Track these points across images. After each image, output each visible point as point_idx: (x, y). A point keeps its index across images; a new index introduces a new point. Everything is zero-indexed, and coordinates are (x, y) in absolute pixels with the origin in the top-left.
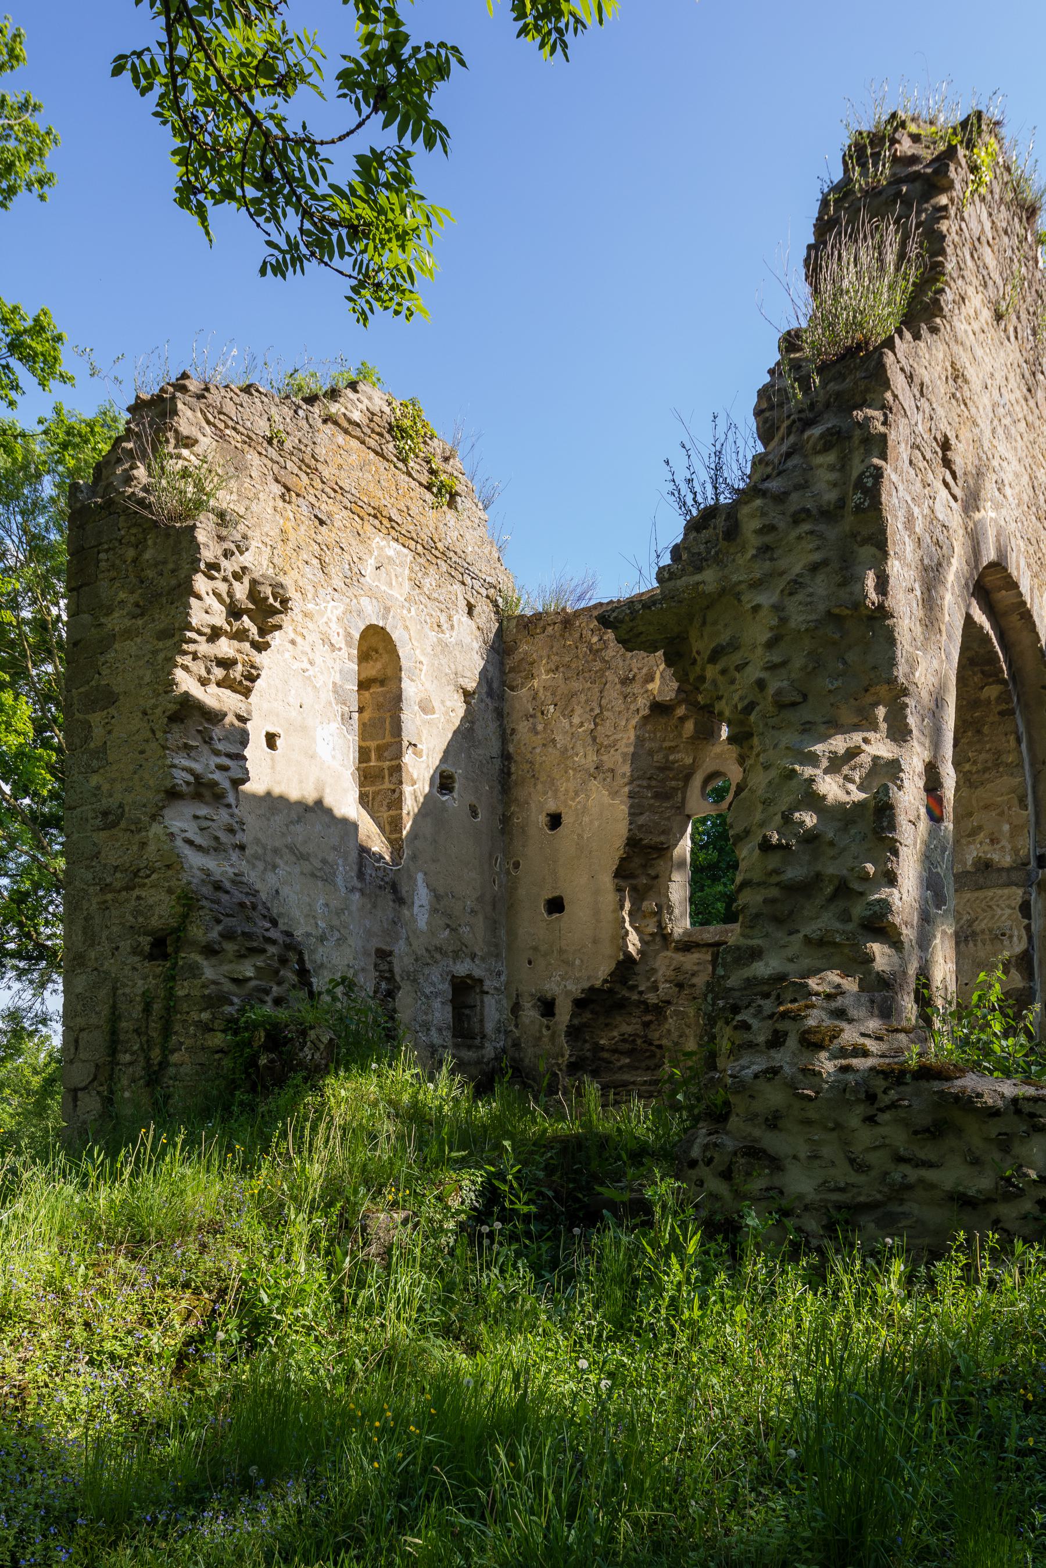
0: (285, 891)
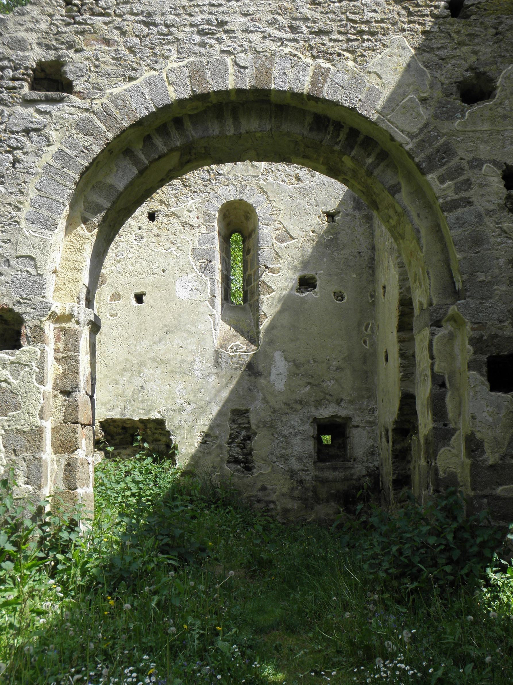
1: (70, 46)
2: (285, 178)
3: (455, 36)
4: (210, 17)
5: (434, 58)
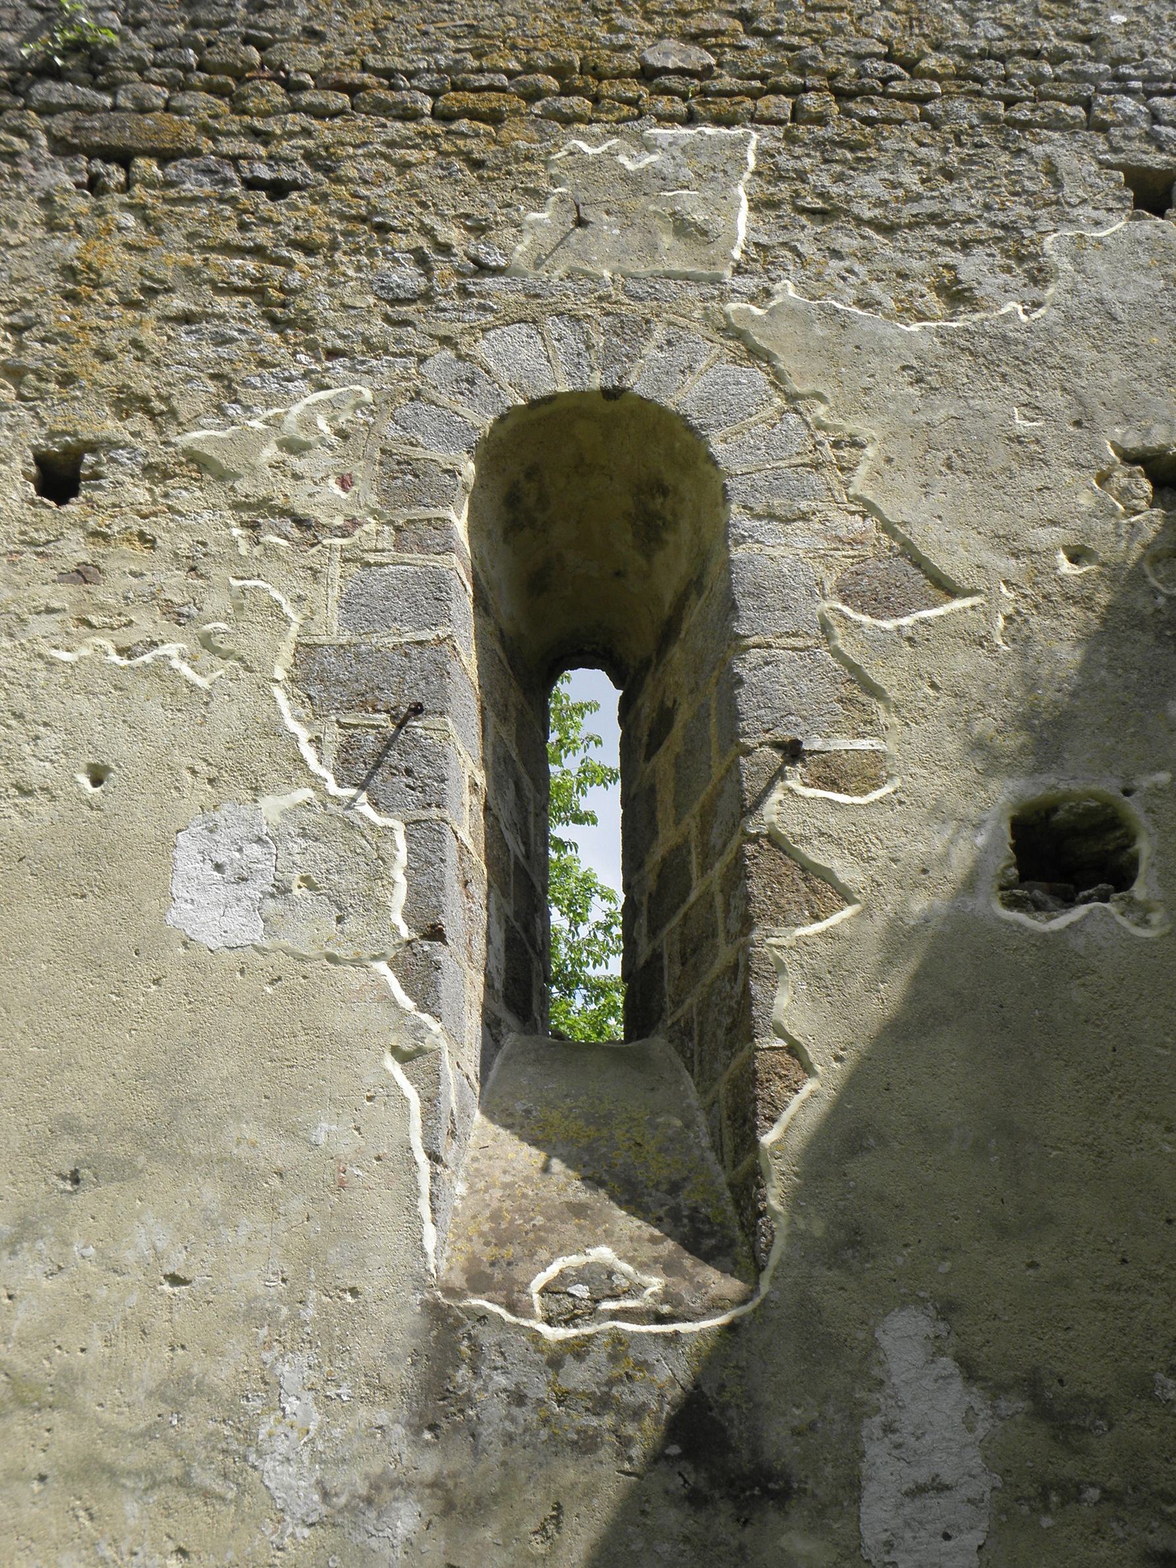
2: (876, 289)
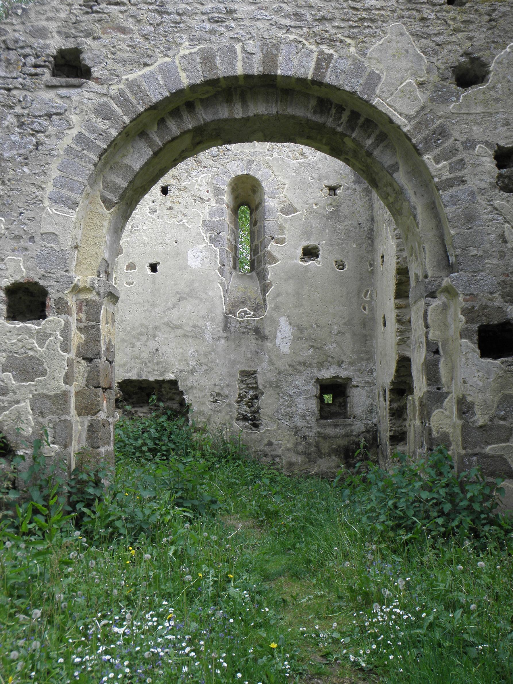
0: (162, 349)
1: (88, 34)
2: (290, 154)
3: (451, 23)
4: (220, 5)
5: (431, 44)
